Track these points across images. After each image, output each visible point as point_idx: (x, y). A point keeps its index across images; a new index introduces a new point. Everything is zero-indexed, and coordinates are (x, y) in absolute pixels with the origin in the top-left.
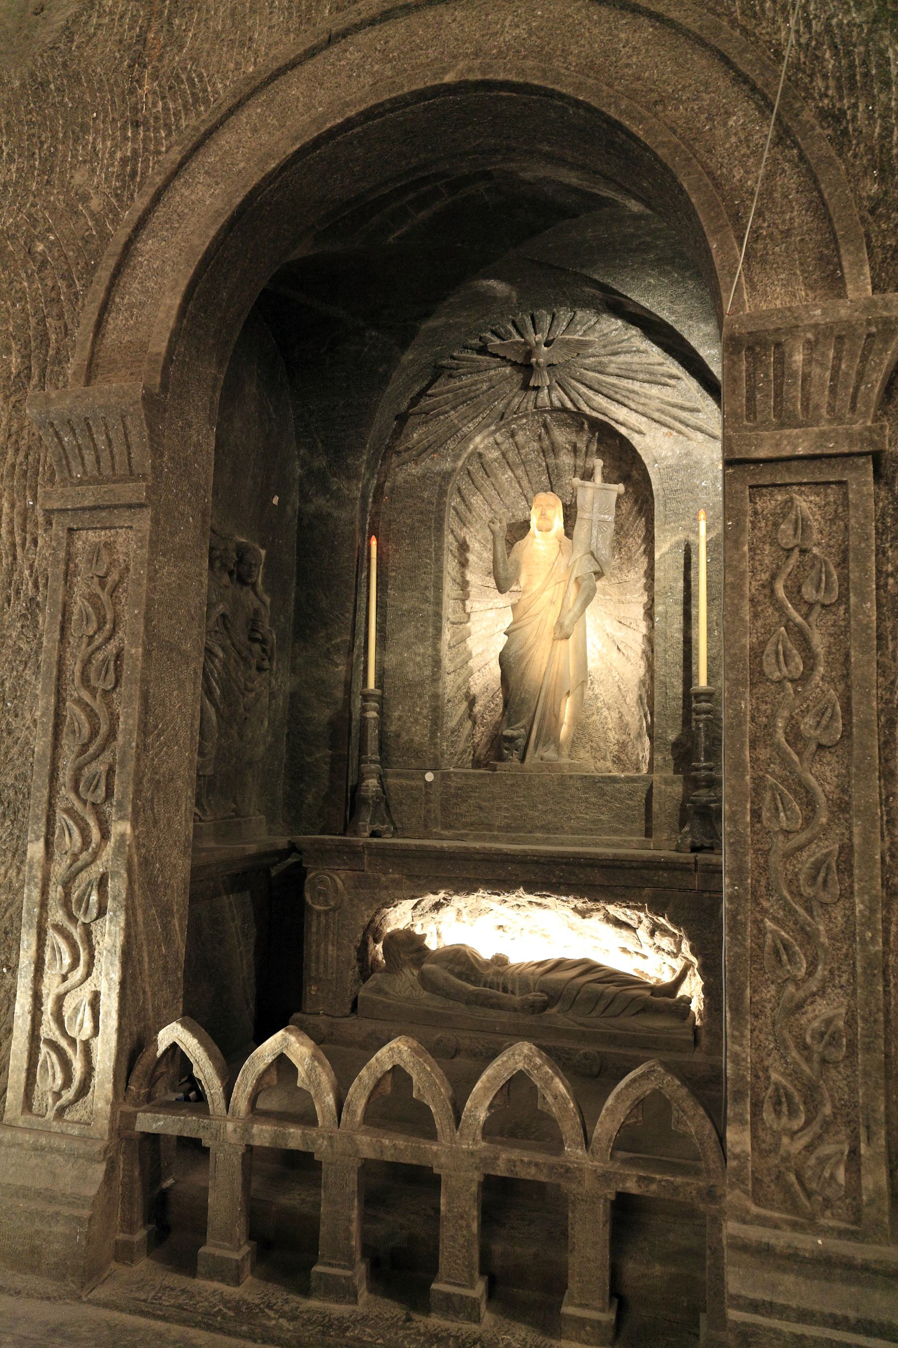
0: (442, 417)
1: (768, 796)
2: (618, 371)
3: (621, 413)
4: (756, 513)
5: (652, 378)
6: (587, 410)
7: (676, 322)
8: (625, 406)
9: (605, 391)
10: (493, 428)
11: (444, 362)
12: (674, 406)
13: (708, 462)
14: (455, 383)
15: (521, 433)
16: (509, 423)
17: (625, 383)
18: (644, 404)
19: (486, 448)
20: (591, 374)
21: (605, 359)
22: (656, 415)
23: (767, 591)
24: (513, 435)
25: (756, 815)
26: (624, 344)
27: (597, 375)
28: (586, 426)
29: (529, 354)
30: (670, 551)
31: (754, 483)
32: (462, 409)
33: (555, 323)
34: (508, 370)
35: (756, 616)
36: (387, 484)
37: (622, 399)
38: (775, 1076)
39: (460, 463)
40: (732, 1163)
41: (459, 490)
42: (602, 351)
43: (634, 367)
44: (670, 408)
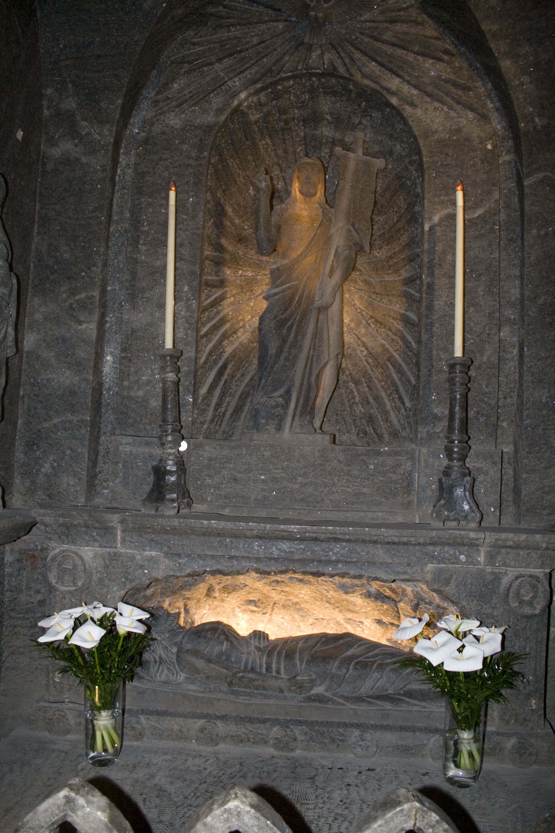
0: (205, 69)
3: (394, 83)
8: (398, 76)
19: (249, 107)
22: (429, 89)
37: (395, 69)
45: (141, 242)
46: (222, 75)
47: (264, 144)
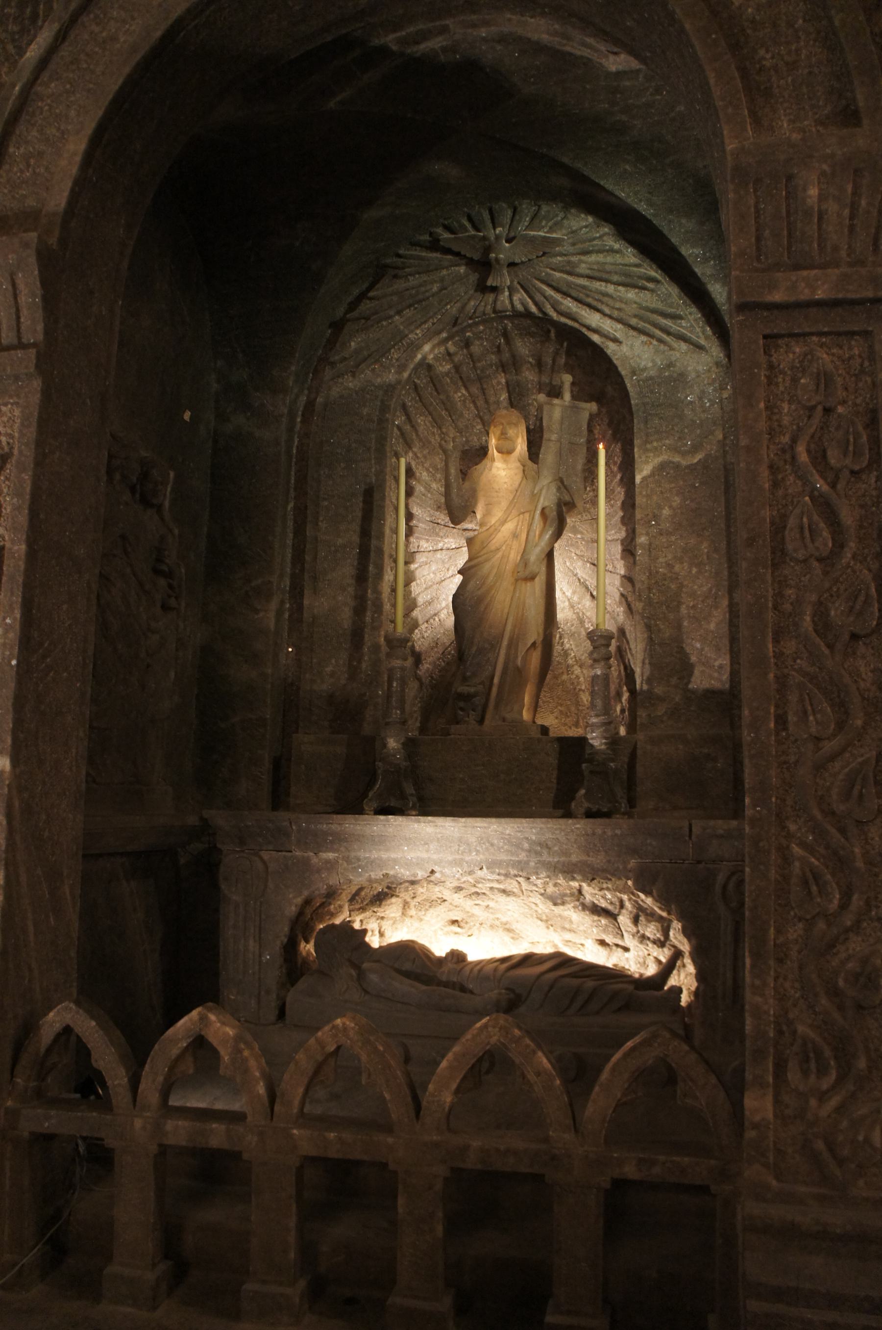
0: (384, 323)
1: (793, 698)
2: (588, 272)
3: (594, 319)
4: (771, 367)
5: (628, 280)
6: (554, 315)
7: (654, 215)
8: (598, 310)
9: (574, 294)
10: (444, 335)
11: (388, 261)
12: (654, 311)
13: (693, 375)
14: (400, 285)
15: (477, 343)
16: (463, 331)
17: (597, 285)
18: (619, 309)
19: (436, 358)
20: (558, 275)
21: (574, 259)
22: (634, 321)
23: (788, 456)
24: (467, 344)
25: (781, 721)
26: (595, 242)
27: (565, 276)
28: (553, 335)
29: (488, 249)
30: (652, 474)
31: (768, 331)
32: (408, 313)
33: (517, 217)
34: (462, 270)
35: (775, 485)
36: (320, 400)
37: (594, 303)
38: (801, 1029)
39: (406, 375)
40: (750, 1134)
41: (404, 407)
42: (571, 249)
43: (608, 268)
44: (649, 314)
45: (321, 519)
46: (402, 327)
47: (459, 395)
